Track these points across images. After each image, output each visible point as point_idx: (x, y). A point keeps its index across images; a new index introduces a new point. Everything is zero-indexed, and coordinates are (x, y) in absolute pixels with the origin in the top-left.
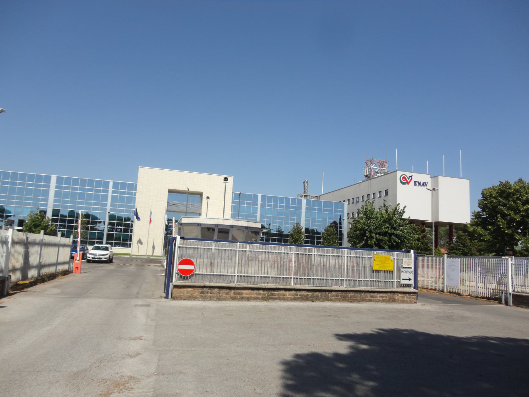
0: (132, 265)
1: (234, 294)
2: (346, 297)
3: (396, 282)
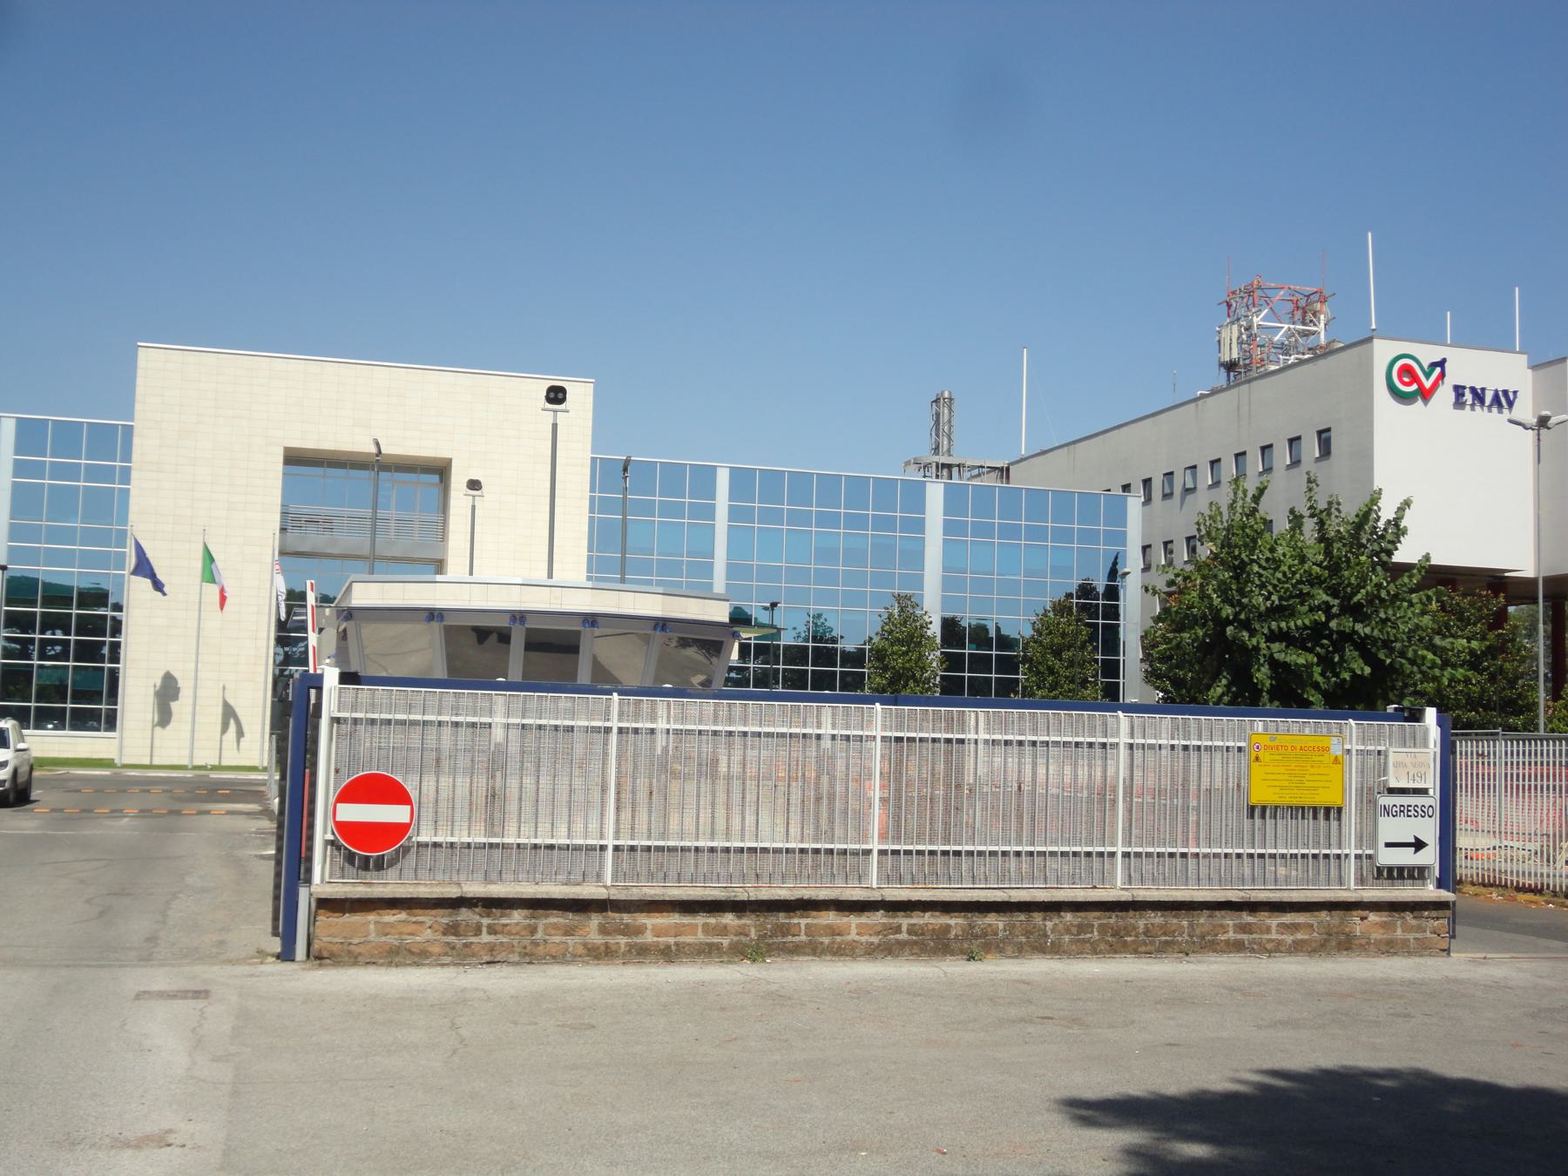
0: (121, 811)
1: (603, 930)
2: (1122, 933)
3: (1358, 857)
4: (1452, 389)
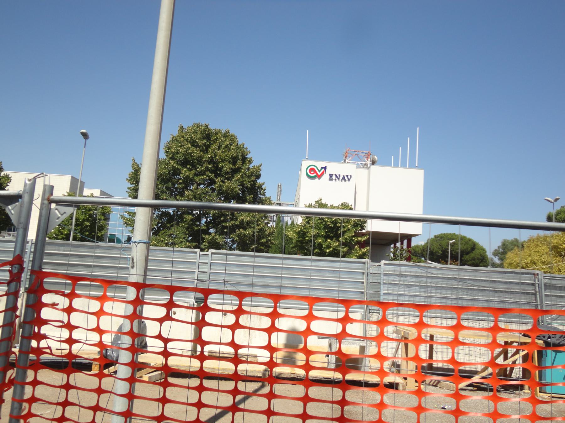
4: (329, 175)
